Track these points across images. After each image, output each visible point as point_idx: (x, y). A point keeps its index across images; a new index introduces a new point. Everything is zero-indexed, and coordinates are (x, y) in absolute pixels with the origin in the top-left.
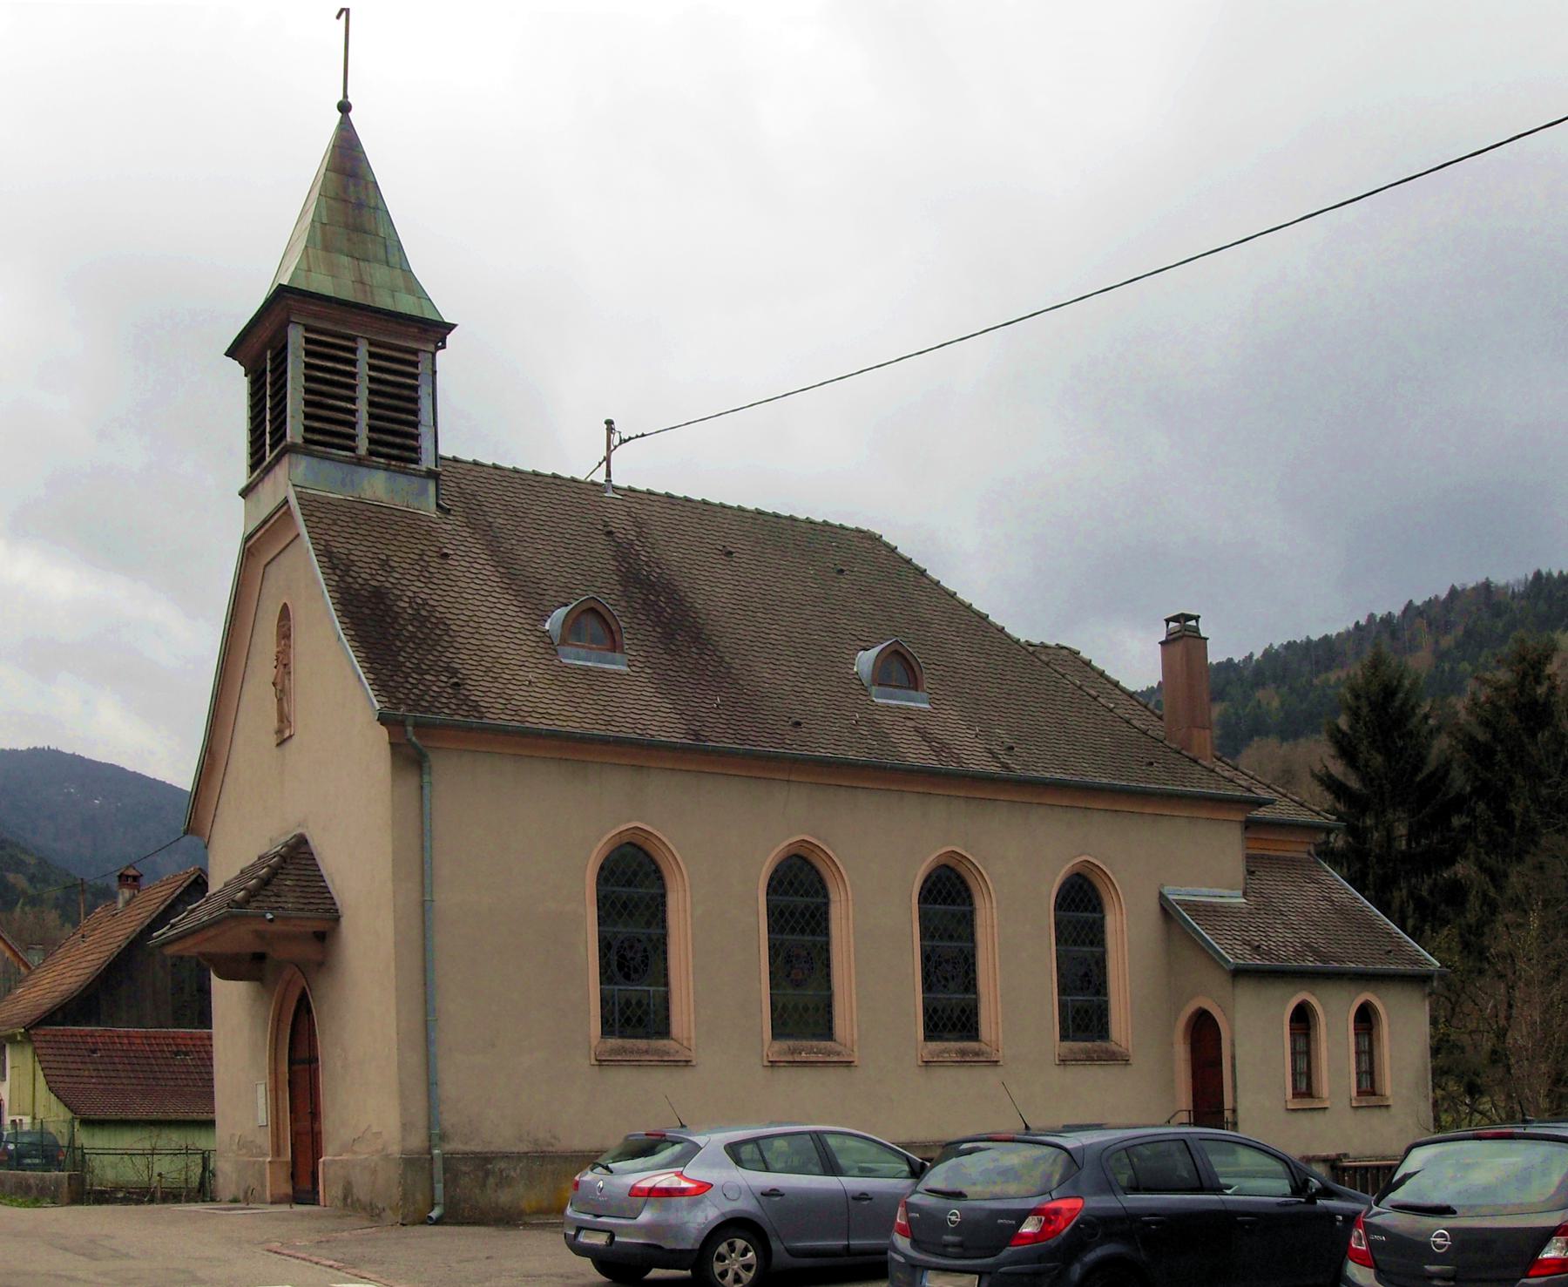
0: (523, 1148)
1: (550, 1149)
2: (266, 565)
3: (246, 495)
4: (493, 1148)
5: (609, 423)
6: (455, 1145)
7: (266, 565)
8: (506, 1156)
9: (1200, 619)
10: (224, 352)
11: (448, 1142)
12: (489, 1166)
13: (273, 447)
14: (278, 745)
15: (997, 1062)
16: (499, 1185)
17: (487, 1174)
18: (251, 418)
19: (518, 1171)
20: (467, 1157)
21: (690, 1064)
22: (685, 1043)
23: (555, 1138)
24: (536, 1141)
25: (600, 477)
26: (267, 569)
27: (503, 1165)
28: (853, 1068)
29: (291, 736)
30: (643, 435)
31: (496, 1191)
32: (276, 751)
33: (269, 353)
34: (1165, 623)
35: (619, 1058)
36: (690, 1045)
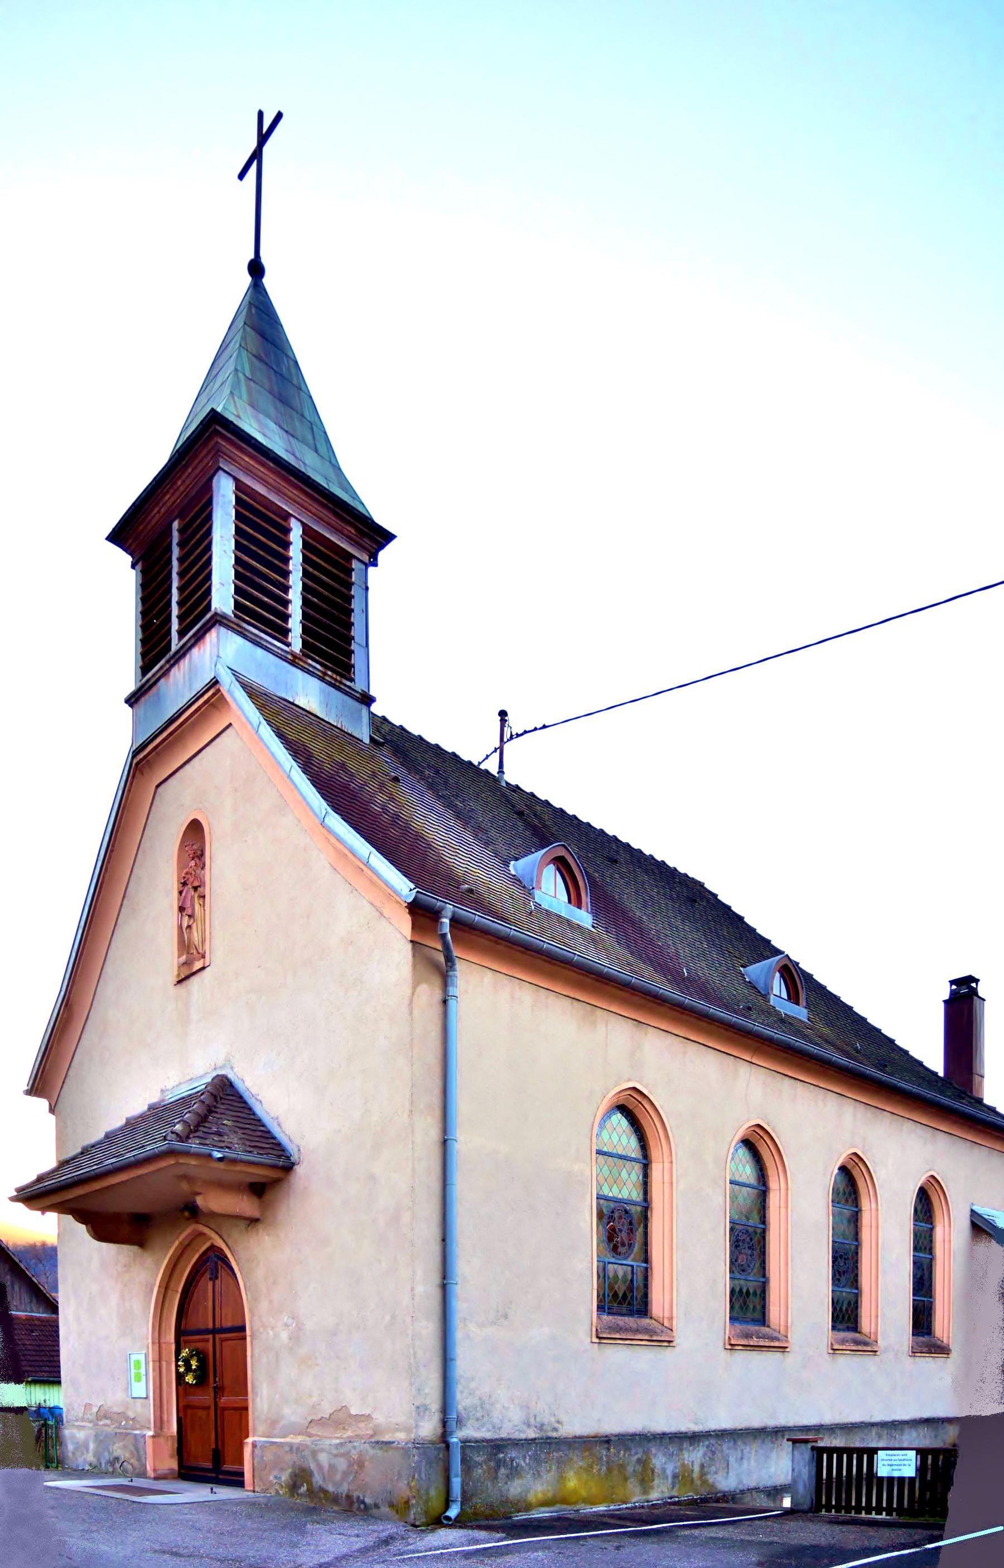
0: (531, 1434)
1: (554, 1434)
2: (158, 786)
3: (137, 701)
4: (504, 1435)
5: (503, 714)
6: (470, 1431)
7: (158, 786)
8: (516, 1443)
9: (979, 983)
10: (106, 535)
11: (461, 1429)
12: (501, 1455)
13: (181, 634)
14: (179, 982)
15: (876, 1351)
16: (510, 1477)
17: (499, 1463)
18: (141, 613)
19: (527, 1461)
20: (480, 1444)
21: (671, 1344)
22: (666, 1324)
23: (558, 1422)
24: (541, 1427)
25: (491, 766)
26: (160, 789)
27: (513, 1454)
28: (786, 1353)
29: (203, 968)
30: (544, 727)
31: (506, 1483)
32: (172, 990)
33: (176, 525)
34: (949, 984)
35: (618, 1336)
36: (672, 1325)
